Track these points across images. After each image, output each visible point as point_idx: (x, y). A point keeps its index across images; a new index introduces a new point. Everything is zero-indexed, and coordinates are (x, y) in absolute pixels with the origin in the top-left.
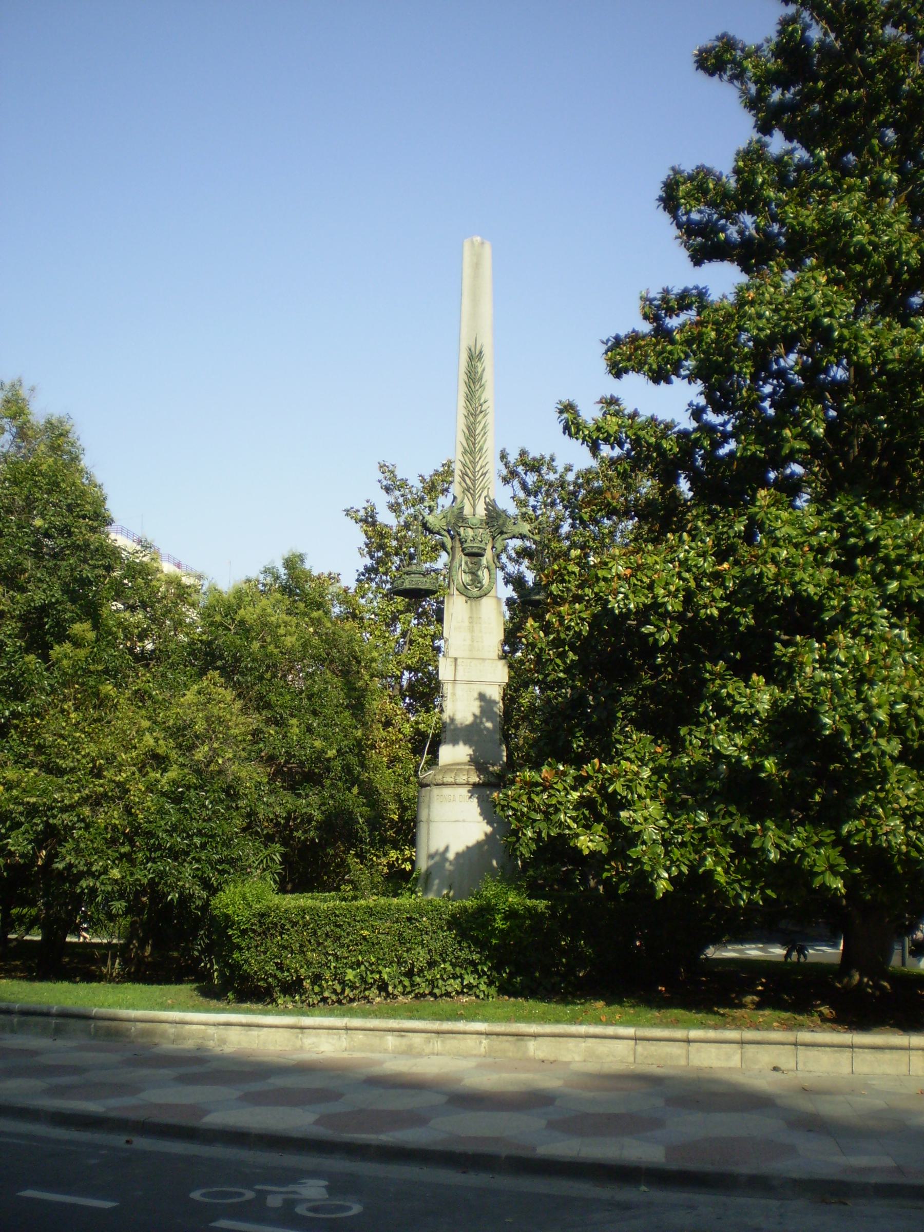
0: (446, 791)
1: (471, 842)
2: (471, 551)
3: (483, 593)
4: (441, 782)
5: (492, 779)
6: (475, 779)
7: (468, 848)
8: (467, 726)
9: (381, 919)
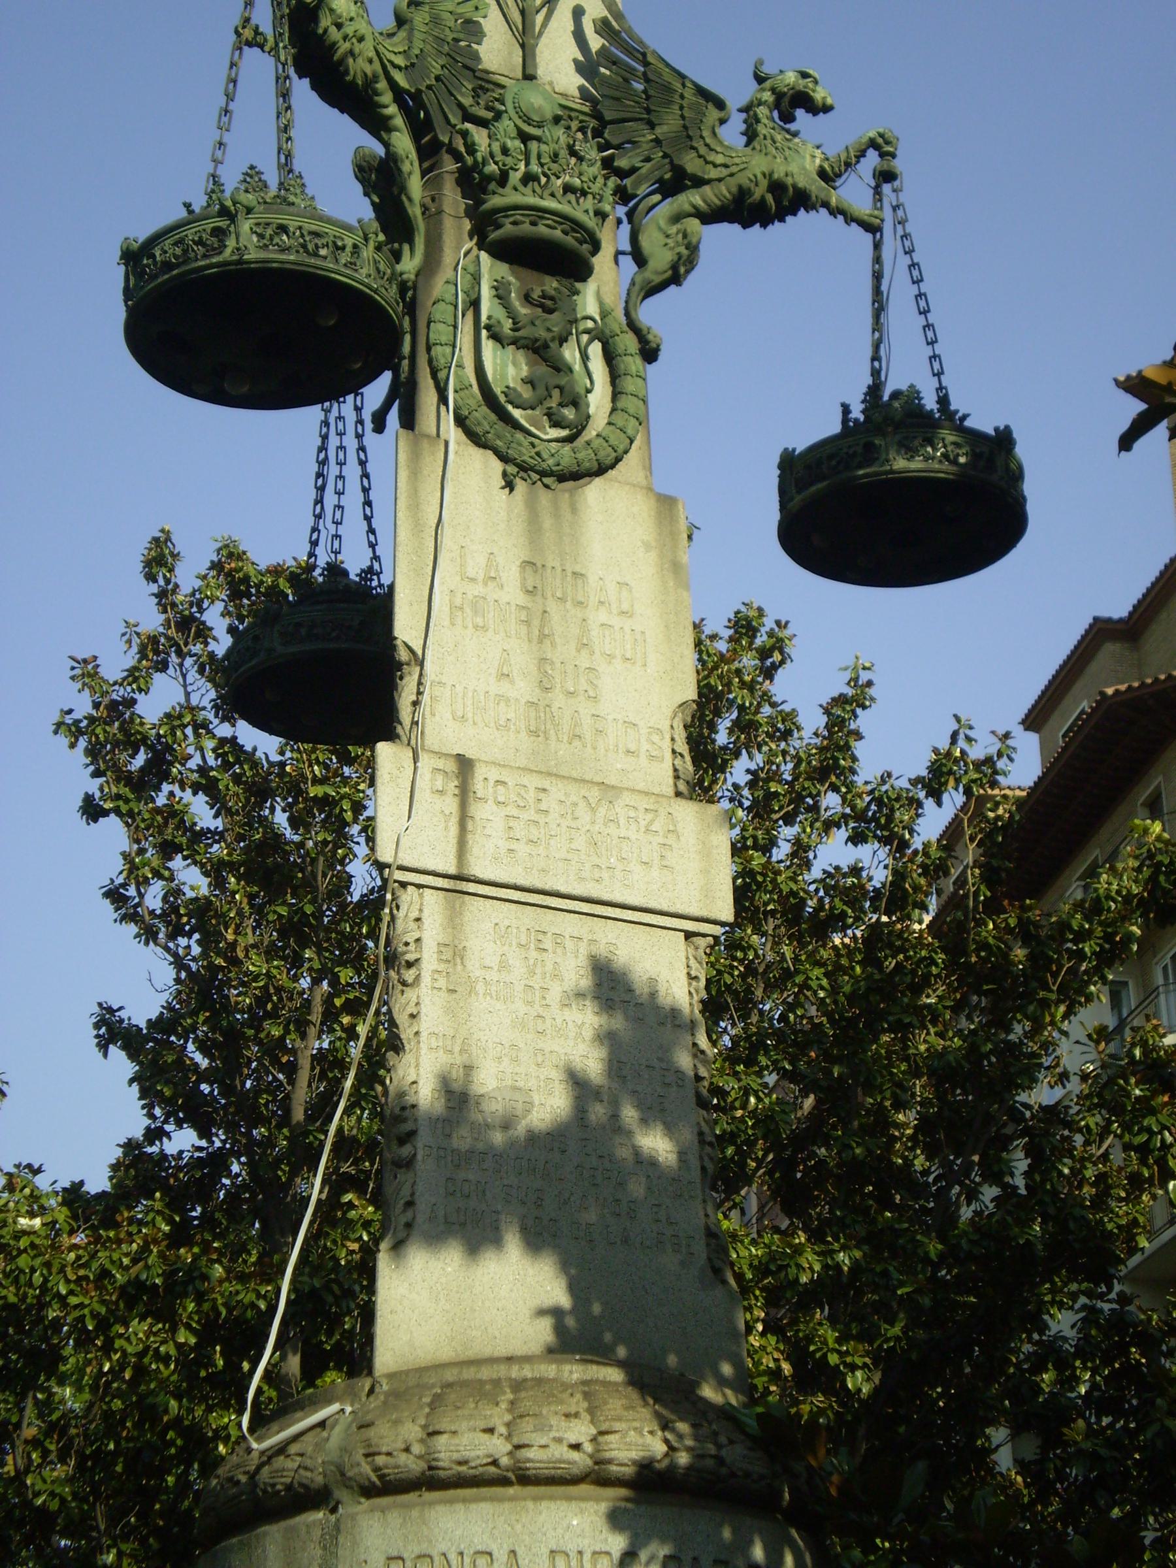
2: (526, 228)
3: (586, 458)
4: (411, 1465)
5: (737, 1454)
6: (638, 1438)
8: (533, 1138)
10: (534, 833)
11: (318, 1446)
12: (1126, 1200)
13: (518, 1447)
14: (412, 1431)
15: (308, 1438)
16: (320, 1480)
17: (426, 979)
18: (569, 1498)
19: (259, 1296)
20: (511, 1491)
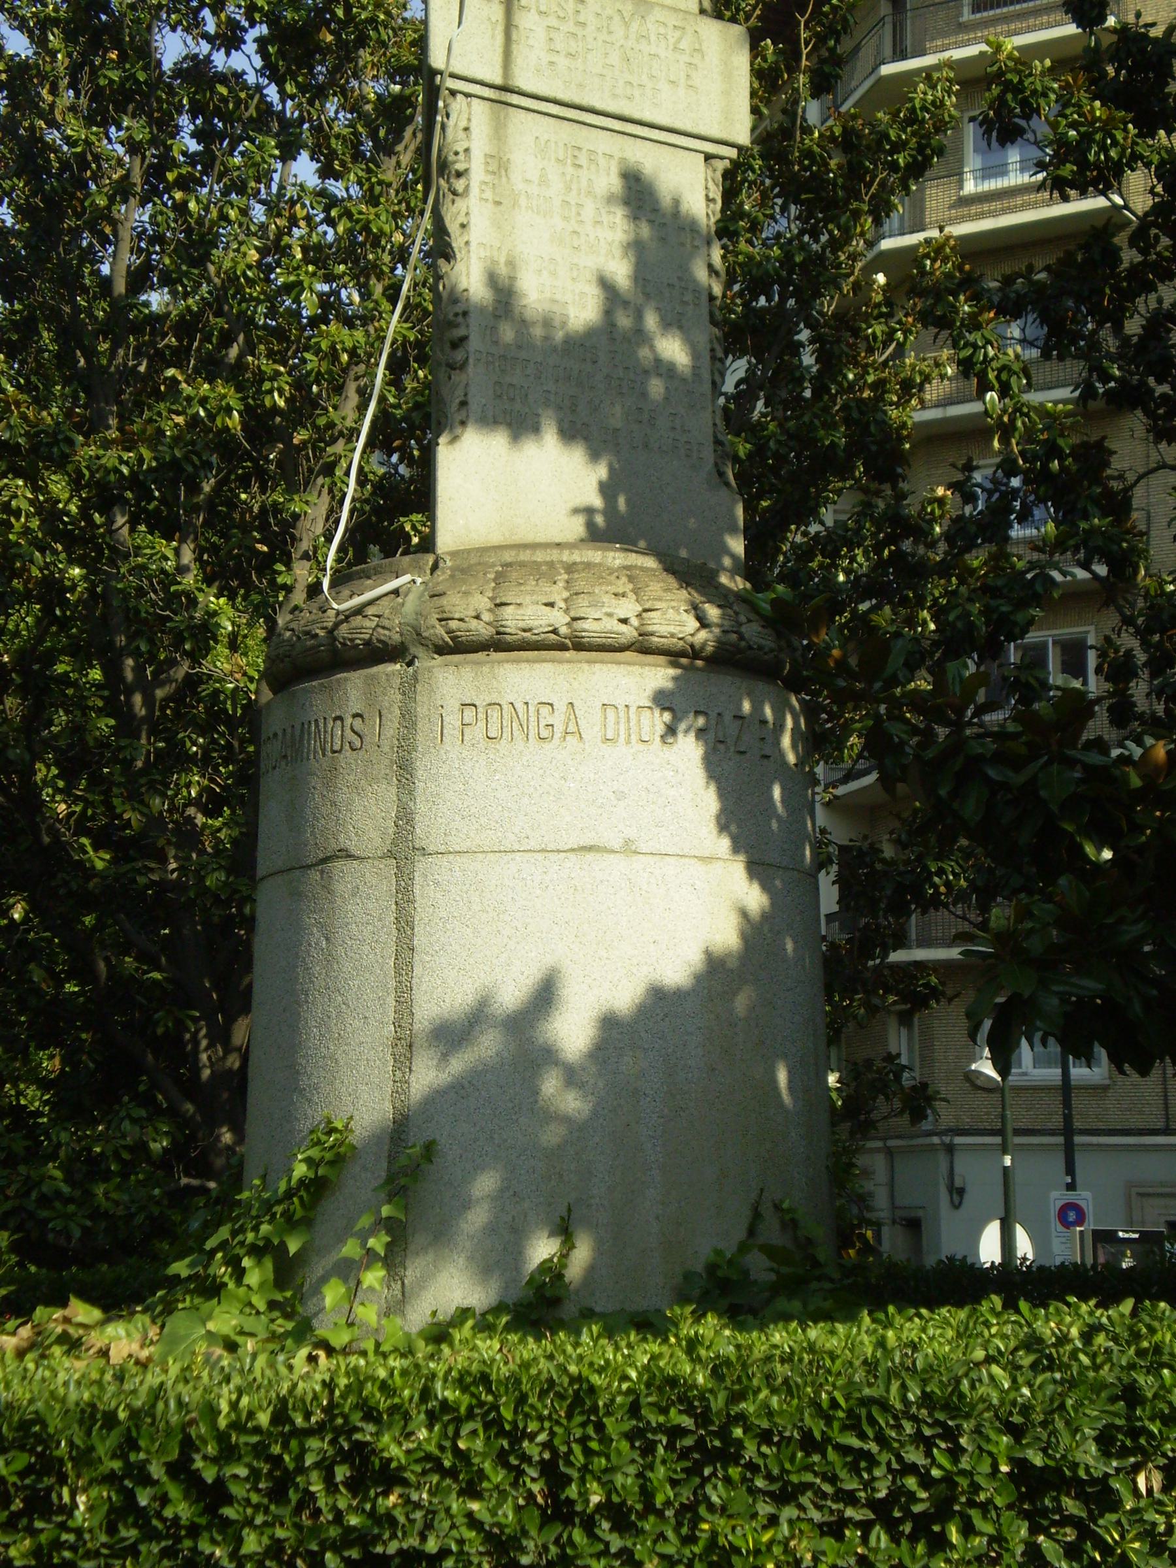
0: (522, 681)
1: (677, 967)
4: (482, 630)
7: (659, 999)
9: (786, 1495)
10: (573, 46)
11: (395, 610)
12: (897, 405)
13: (574, 619)
14: (481, 602)
15: (384, 602)
16: (397, 638)
17: (475, 191)
18: (619, 663)
19: (122, 461)
20: (567, 655)
